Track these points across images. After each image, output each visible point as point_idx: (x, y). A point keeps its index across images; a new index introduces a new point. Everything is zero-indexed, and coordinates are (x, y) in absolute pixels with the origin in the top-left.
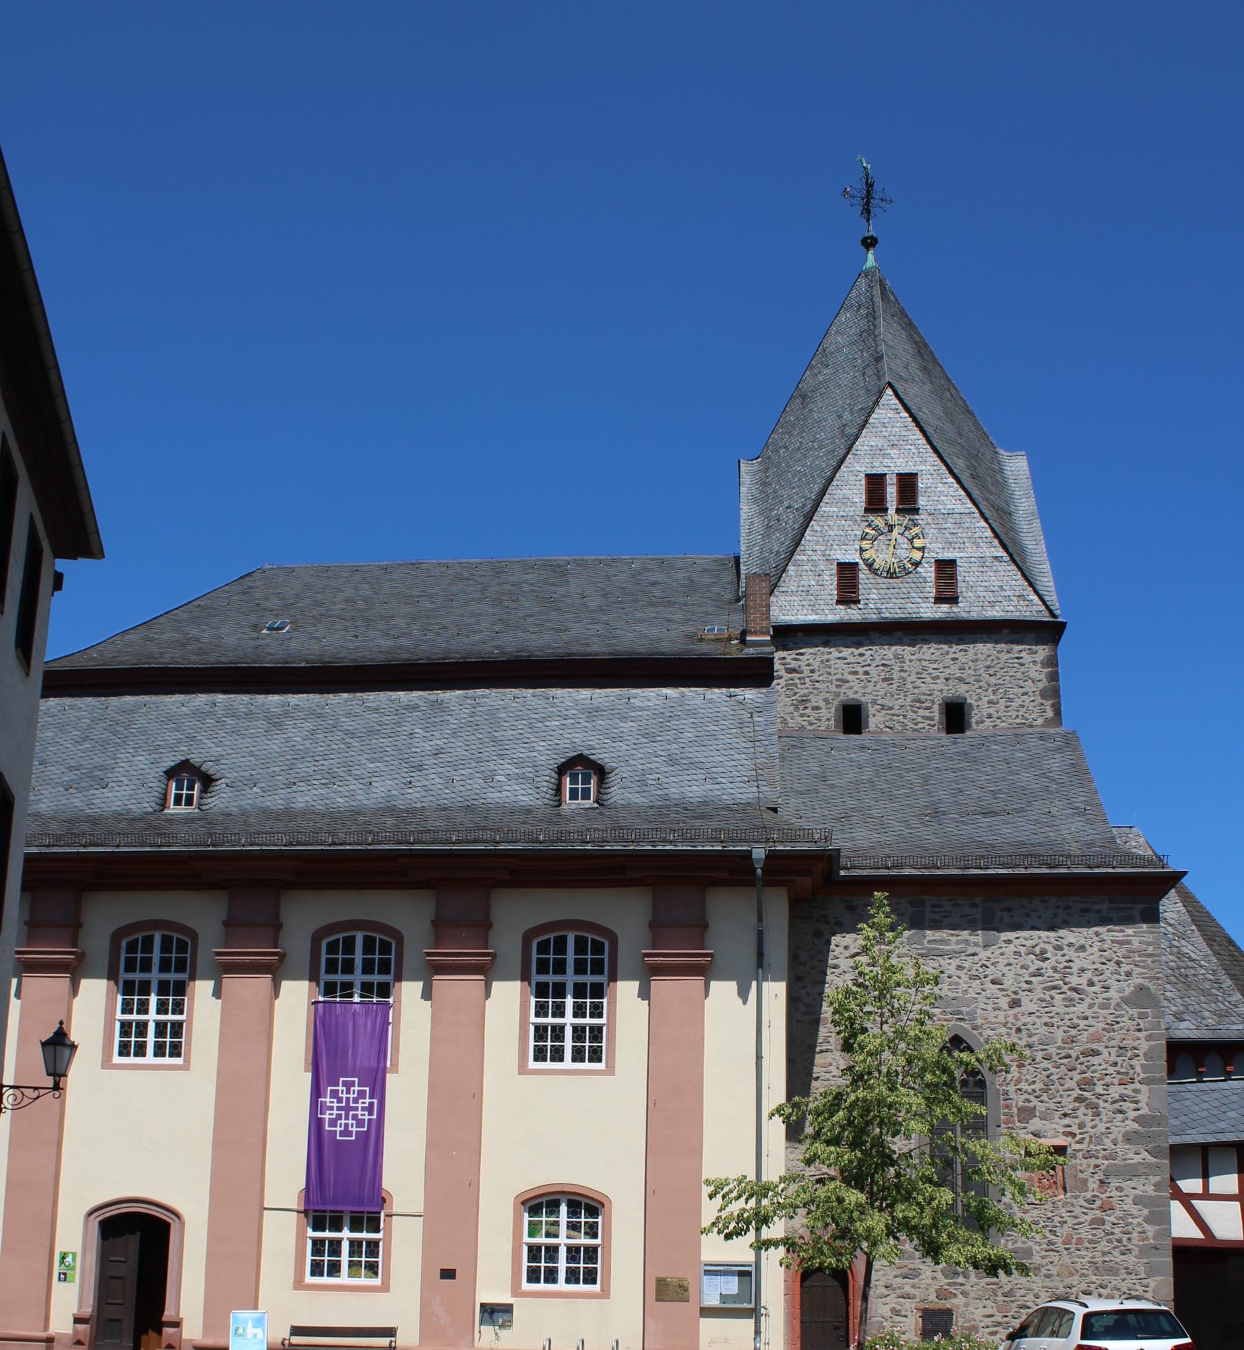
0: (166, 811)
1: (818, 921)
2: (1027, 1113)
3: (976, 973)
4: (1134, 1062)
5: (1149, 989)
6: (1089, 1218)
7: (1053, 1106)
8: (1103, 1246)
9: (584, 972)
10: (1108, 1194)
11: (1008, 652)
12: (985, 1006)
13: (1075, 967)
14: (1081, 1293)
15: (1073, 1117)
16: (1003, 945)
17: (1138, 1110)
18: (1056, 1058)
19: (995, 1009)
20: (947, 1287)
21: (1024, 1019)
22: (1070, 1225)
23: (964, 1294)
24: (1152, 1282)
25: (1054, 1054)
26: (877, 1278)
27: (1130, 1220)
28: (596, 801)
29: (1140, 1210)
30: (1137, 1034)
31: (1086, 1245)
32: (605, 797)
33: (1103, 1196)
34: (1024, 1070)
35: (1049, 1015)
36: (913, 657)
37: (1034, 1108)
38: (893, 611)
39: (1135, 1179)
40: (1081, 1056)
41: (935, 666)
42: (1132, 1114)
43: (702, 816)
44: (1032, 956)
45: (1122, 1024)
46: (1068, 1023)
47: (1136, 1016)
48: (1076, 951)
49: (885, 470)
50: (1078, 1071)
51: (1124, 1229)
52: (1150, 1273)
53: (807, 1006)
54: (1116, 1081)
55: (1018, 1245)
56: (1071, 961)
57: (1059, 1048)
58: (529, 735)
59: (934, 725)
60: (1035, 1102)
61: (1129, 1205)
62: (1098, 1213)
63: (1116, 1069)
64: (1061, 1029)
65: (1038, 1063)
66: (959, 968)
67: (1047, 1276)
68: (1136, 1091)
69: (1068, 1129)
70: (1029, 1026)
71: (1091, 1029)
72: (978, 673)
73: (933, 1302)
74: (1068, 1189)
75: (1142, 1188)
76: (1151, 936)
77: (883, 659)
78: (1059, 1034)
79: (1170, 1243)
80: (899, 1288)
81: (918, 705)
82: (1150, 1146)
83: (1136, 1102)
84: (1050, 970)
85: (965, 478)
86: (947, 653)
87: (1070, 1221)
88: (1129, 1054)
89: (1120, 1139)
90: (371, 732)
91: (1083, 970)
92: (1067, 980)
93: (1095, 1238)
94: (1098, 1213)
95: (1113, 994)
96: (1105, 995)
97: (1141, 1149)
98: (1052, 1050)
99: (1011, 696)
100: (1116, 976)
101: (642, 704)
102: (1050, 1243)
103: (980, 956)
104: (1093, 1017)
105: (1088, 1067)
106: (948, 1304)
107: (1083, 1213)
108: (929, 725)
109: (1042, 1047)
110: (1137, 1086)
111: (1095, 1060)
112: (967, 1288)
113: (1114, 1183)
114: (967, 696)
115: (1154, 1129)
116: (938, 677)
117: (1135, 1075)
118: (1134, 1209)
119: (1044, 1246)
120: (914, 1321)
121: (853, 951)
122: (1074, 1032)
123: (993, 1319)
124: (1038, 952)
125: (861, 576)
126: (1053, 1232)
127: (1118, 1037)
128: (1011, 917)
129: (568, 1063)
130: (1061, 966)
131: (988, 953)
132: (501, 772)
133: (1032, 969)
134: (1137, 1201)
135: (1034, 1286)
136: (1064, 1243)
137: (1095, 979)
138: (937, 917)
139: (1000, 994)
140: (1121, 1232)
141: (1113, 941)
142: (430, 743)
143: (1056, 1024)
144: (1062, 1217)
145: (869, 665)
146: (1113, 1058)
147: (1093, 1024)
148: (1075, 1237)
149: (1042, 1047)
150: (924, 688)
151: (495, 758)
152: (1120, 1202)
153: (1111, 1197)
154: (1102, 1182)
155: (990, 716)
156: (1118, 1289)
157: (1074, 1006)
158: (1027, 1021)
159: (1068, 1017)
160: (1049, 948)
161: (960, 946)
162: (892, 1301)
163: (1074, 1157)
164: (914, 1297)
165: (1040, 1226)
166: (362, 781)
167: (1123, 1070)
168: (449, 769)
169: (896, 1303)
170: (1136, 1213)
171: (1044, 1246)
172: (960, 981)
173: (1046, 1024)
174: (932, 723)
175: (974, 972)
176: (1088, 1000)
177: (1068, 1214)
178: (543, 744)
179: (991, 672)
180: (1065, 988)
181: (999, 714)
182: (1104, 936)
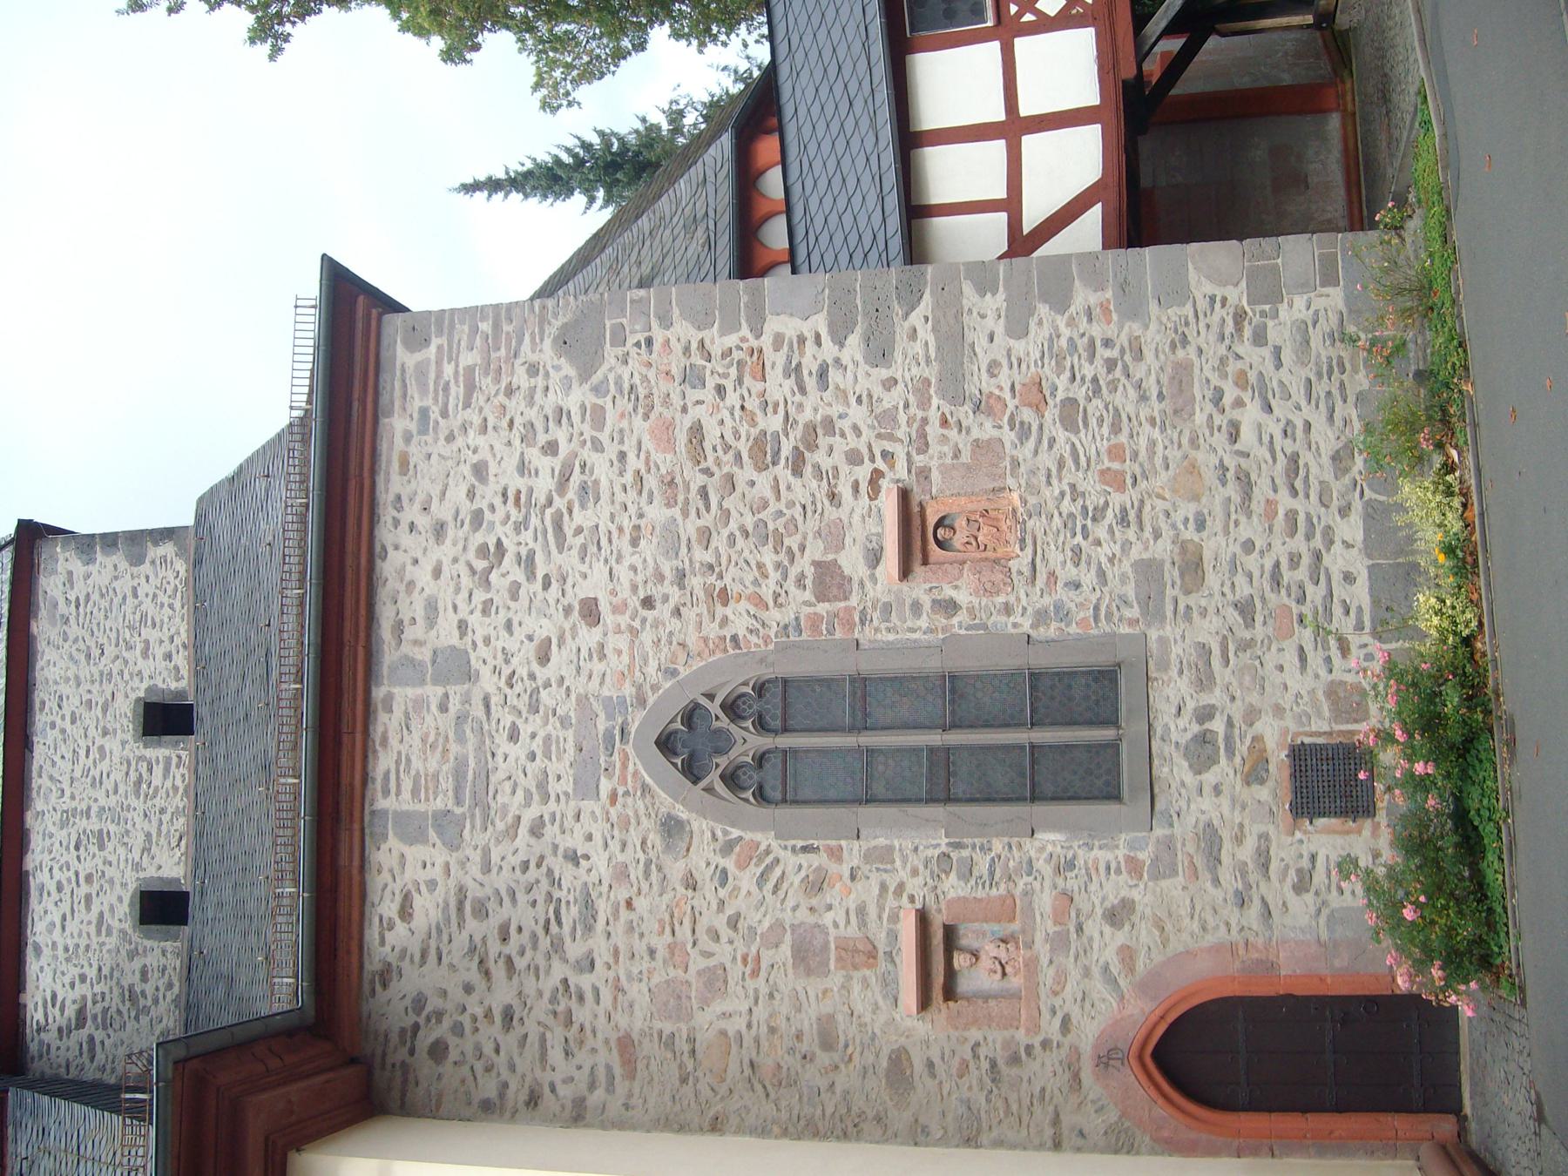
1: (412, 1052)
2: (829, 581)
3: (526, 697)
4: (716, 351)
5: (565, 326)
6: (1061, 435)
7: (812, 524)
8: (1125, 399)
10: (1007, 395)
12: (596, 680)
13: (517, 483)
14: (1237, 446)
15: (836, 477)
16: (468, 639)
17: (818, 337)
18: (707, 520)
19: (602, 657)
20: (1238, 760)
21: (625, 593)
22: (1080, 474)
23: (1252, 715)
24: (1201, 287)
25: (700, 523)
26: (1223, 928)
27: (1063, 342)
29: (1040, 323)
30: (657, 346)
31: (1123, 438)
33: (1011, 404)
34: (734, 589)
35: (615, 535)
36: (68, 793)
37: (817, 564)
39: (969, 339)
40: (703, 465)
41: (82, 753)
42: (829, 350)
44: (494, 577)
45: (637, 380)
46: (632, 494)
47: (620, 351)
50: (735, 469)
51: (1084, 355)
53: (592, 1086)
54: (757, 386)
55: (1131, 595)
56: (504, 494)
57: (685, 514)
59: (179, 757)
60: (804, 565)
61: (1027, 348)
62: (1051, 413)
63: (729, 388)
64: (646, 509)
65: (718, 556)
66: (514, 736)
67: (1201, 525)
68: (778, 341)
69: (863, 487)
70: (640, 578)
71: (648, 444)
72: (97, 676)
73: (1275, 790)
74: (996, 485)
75: (990, 323)
77: (68, 848)
78: (657, 513)
80: (1244, 874)
81: (144, 786)
83: (802, 340)
84: (521, 538)
86: (63, 731)
88: (699, 361)
89: (884, 373)
91: (523, 468)
92: (543, 500)
94: (1051, 413)
95: (575, 399)
96: (576, 418)
98: (690, 527)
102: (1123, 520)
103: (491, 689)
104: (622, 442)
106: (1279, 758)
107: (1051, 447)
108: (178, 767)
109: (684, 550)
110: (766, 341)
113: (979, 382)
114: (133, 696)
115: (858, 302)
116: (101, 748)
117: (745, 346)
118: (1038, 335)
119: (1131, 534)
120: (1324, 838)
121: (474, 976)
122: (651, 482)
123: (1309, 647)
126: (1098, 514)
127: (664, 386)
130: (514, 512)
131: (485, 672)
133: (518, 575)
134: (1018, 330)
135: (1225, 557)
136: (1121, 488)
137: (542, 439)
138: (407, 785)
139: (571, 644)
140: (1091, 362)
141: (467, 405)
143: (635, 521)
144: (1063, 494)
146: (708, 394)
147: (634, 442)
148: (1107, 464)
149: (684, 550)
150: (117, 776)
152: (1024, 366)
153: (1013, 386)
155: (168, 657)
156: (1223, 361)
157: (596, 482)
158: (627, 585)
159: (620, 497)
160: (478, 538)
161: (468, 731)
163: (924, 474)
164: (1264, 837)
165: (1084, 544)
167: (733, 371)
169: (1282, 880)
170: (1046, 331)
171: (1131, 534)
172: (541, 734)
173: (635, 542)
174: (175, 760)
175: (522, 705)
176: (587, 454)
177: (1055, 481)
179: (96, 652)
180: (559, 503)
181: (166, 639)
182: (455, 423)
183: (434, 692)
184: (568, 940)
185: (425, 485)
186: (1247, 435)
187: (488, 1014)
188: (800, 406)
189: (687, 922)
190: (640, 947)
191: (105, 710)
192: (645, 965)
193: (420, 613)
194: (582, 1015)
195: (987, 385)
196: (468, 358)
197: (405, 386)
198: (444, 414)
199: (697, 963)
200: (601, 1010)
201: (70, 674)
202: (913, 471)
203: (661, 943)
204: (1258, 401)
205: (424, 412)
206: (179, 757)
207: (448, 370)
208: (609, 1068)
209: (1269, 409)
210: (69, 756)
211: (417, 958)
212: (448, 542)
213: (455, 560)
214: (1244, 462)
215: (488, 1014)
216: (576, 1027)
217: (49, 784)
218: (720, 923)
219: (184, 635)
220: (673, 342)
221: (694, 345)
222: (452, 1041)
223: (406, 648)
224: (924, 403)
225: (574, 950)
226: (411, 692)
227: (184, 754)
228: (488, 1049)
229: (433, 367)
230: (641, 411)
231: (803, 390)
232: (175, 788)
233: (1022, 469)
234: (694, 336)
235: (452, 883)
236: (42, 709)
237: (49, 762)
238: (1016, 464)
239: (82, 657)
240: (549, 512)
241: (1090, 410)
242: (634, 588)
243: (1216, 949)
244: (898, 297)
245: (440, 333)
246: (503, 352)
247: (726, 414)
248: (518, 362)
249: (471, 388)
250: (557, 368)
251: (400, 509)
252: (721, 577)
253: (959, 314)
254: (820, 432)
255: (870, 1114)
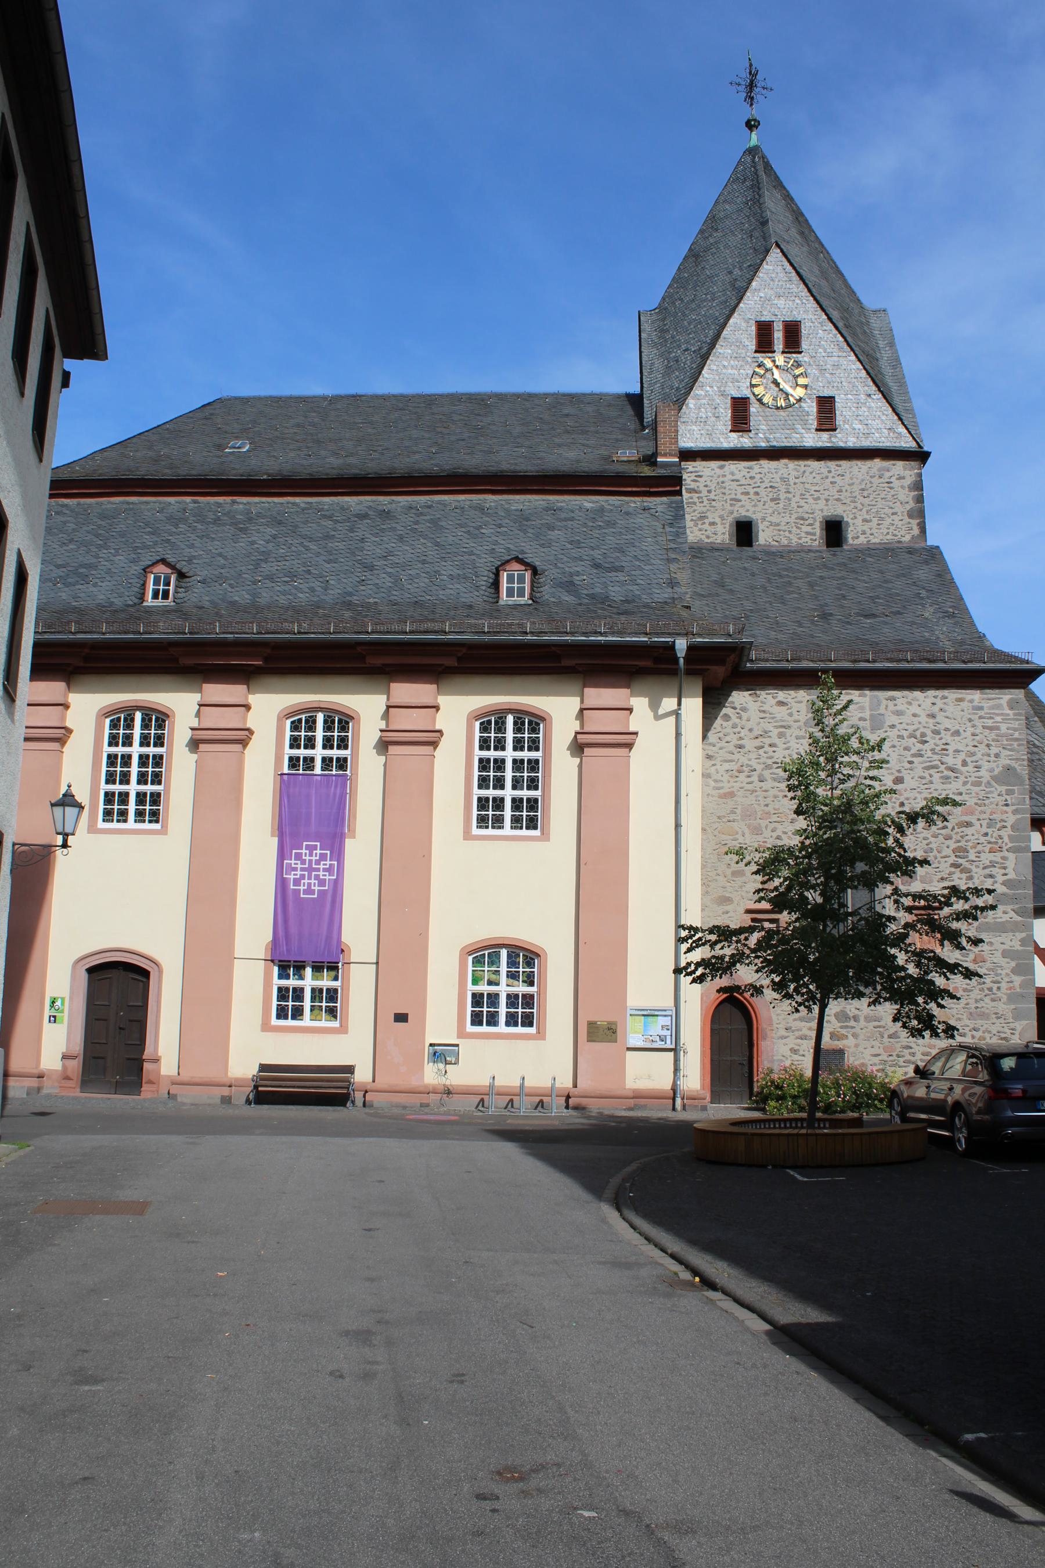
0: (145, 604)
4: (1001, 833)
5: (1015, 769)
9: (522, 749)
11: (880, 477)
13: (951, 749)
16: (888, 729)
17: (1006, 874)
20: (839, 1030)
21: (906, 795)
23: (855, 1035)
24: (1019, 1025)
27: (1000, 971)
28: (531, 598)
29: (1008, 963)
30: (1005, 808)
32: (538, 595)
35: (929, 791)
36: (797, 481)
38: (781, 440)
39: (1002, 934)
41: (817, 488)
42: (1000, 879)
43: (626, 613)
47: (1004, 792)
48: (952, 735)
49: (773, 318)
50: (954, 840)
53: (716, 781)
54: (987, 850)
56: (946, 744)
58: (468, 541)
59: (815, 540)
61: (998, 958)
63: (986, 838)
68: (1004, 858)
70: (912, 802)
72: (854, 495)
76: (1017, 723)
77: (770, 482)
79: (1034, 991)
80: (798, 1030)
81: (802, 522)
82: (1017, 906)
83: (1005, 868)
84: (928, 751)
85: (840, 325)
86: (827, 477)
88: (999, 825)
90: (328, 537)
92: (943, 760)
93: (969, 987)
95: (984, 773)
96: (977, 774)
99: (883, 516)
100: (986, 758)
101: (567, 516)
105: (962, 837)
108: (811, 539)
110: (1005, 854)
111: (969, 831)
112: (857, 1030)
116: (818, 498)
117: (1004, 845)
118: (1003, 962)
121: (756, 733)
123: (880, 1058)
124: (918, 736)
125: (752, 409)
127: (988, 811)
128: (895, 705)
129: (507, 830)
130: (939, 748)
132: (444, 573)
134: (1005, 954)
137: (968, 760)
141: (984, 727)
142: (380, 547)
145: (759, 487)
146: (984, 830)
147: (967, 799)
150: (806, 508)
151: (438, 560)
155: (864, 533)
156: (990, 1032)
157: (950, 783)
158: (908, 796)
160: (928, 732)
162: (792, 1042)
166: (321, 580)
167: (993, 840)
168: (398, 569)
174: (814, 538)
176: (962, 779)
178: (480, 548)
179: (865, 493)
180: (942, 768)
181: (872, 531)
182: (977, 722)
183: (867, 714)
184: (771, 771)
185: (951, 709)
187: (741, 738)
188: (977, 867)
189: (779, 819)
190: (768, 801)
191: (838, 500)
192: (762, 803)
193: (899, 708)
194: (742, 777)
196: (1003, 728)
197: (993, 699)
198: (980, 717)
199: (763, 823)
200: (744, 784)
201: (855, 480)
203: (770, 809)
205: (981, 708)
206: (815, 540)
207: (999, 719)
208: (722, 788)
210: (815, 481)
211: (762, 709)
212: (927, 720)
213: (920, 723)
215: (741, 738)
216: (737, 774)
217: (802, 470)
218: (779, 833)
219: (873, 541)
220: (1007, 815)
221: (1005, 824)
222: (730, 723)
223: (885, 702)
225: (767, 774)
226: (867, 705)
227: (817, 542)
228: (728, 738)
229: (1001, 712)
230: (979, 802)
231: (984, 868)
232: (800, 538)
234: (1008, 825)
235: (792, 723)
236: (837, 465)
237: (811, 470)
239: (863, 486)
240: (939, 763)
242: (907, 799)
243: (770, 1019)
244: (1021, 907)
245: (1015, 714)
246: (1005, 742)
247: (976, 836)
248: (1001, 749)
249: (991, 728)
250: (998, 766)
251: (941, 699)
252: (912, 834)
254: (968, 875)
255: (709, 889)
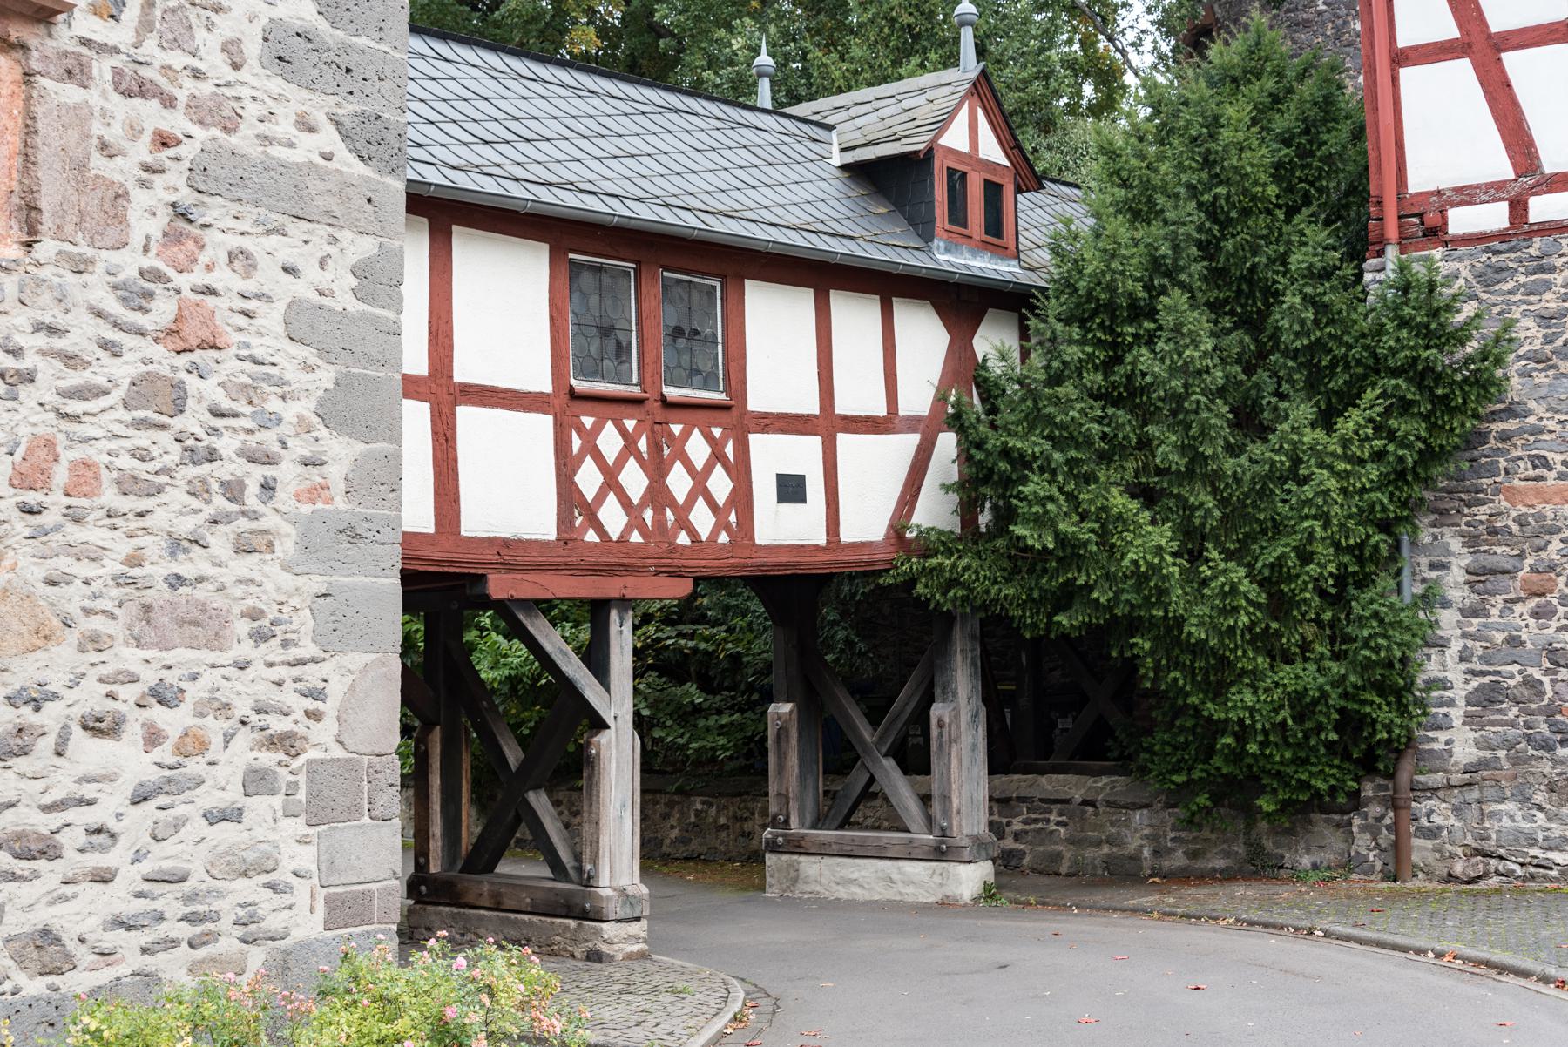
6: (125, 370)
10: (199, 277)
14: (77, 730)
22: (50, 397)
27: (274, 405)
29: (308, 368)
31: (110, 497)
33: (183, 281)
39: (297, 229)
51: (252, 441)
52: (333, 639)
74: (47, 222)
75: (311, 272)
87: (49, 375)
93: (141, 469)
94: (164, 360)
97: (319, 107)
107: (105, 345)
115: (362, 41)
118: (289, 359)
140: (241, 453)
144: (16, 352)
148: (67, 456)
152: (242, 321)
153: (211, 292)
154: (181, 214)
170: (292, 374)
177: (42, 340)
186: (90, 752)
195: (218, 244)
202: (84, 50)
204: (154, 775)
209: (140, 799)
214: (46, 745)
224: (200, 112)
233: (71, 278)
238: (80, 267)
241: (165, 438)
244: (364, 117)
253: (332, 220)
